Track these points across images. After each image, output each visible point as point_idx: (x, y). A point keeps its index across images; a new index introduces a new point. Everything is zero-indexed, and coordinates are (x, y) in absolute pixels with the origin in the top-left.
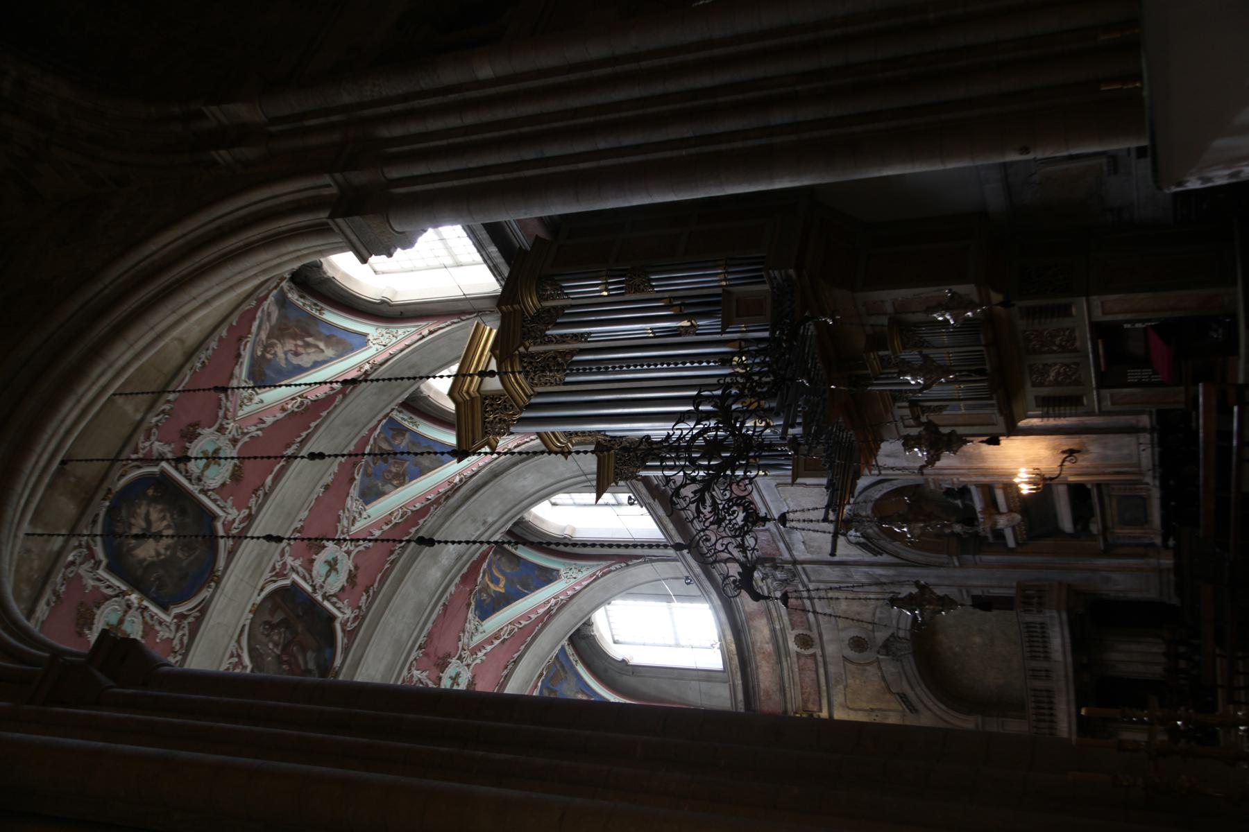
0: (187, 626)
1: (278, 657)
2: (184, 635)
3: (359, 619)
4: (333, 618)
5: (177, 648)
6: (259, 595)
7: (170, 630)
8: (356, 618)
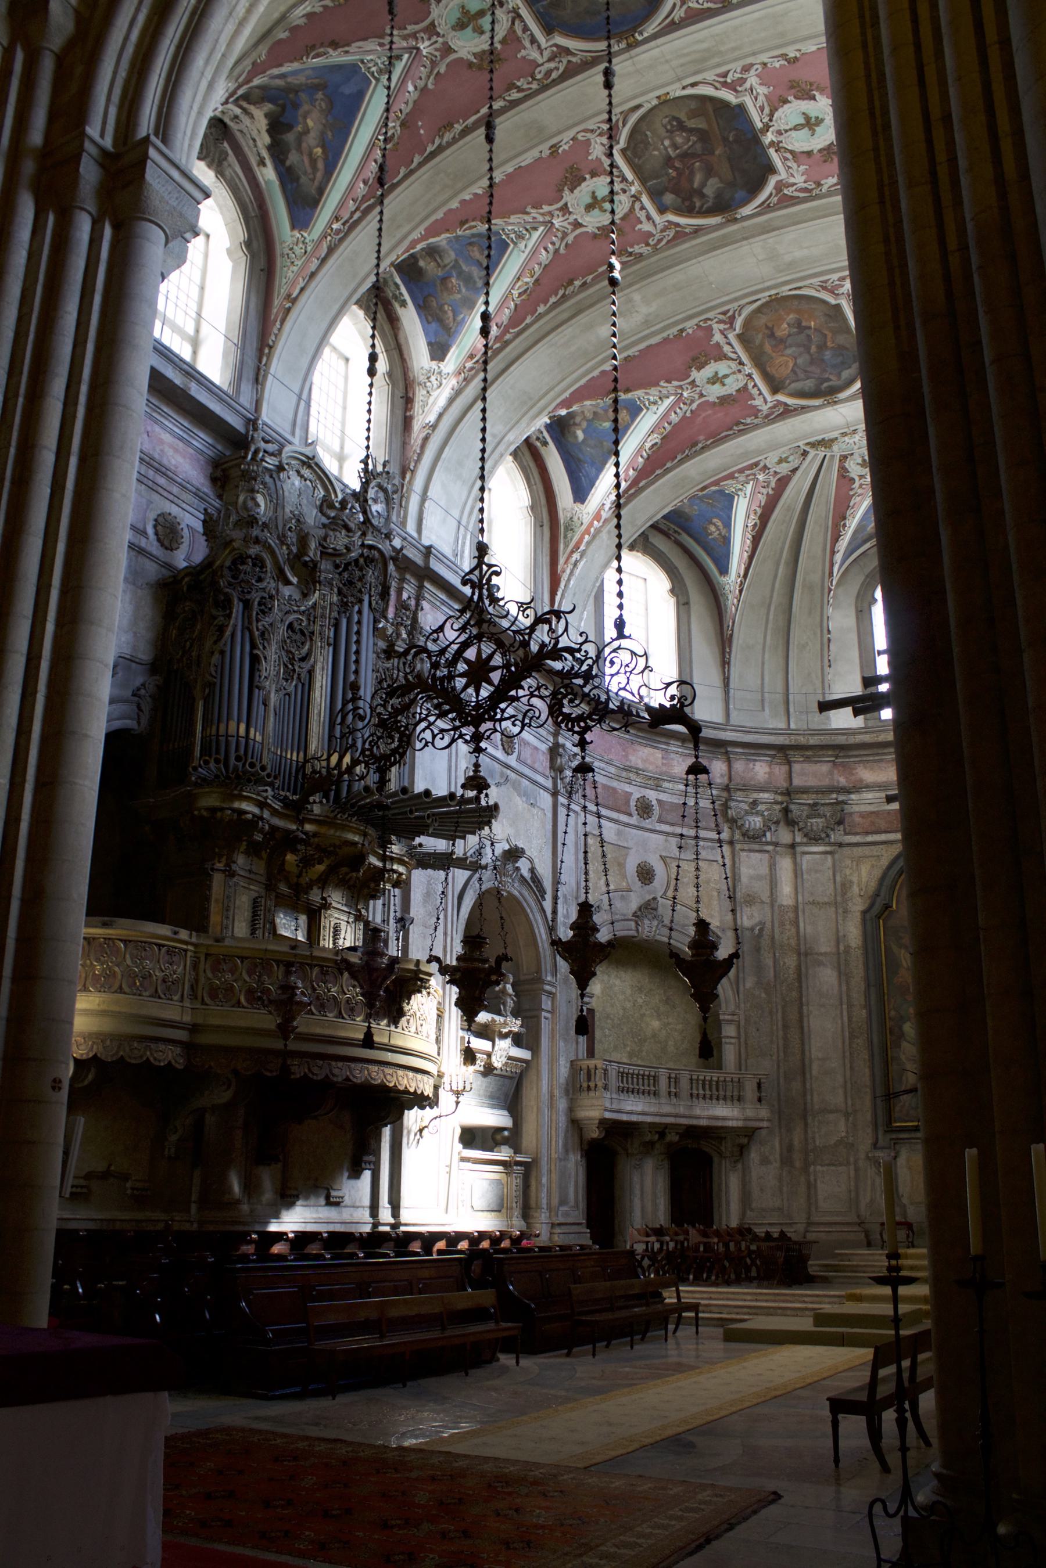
0: (565, 62)
2: (557, 69)
4: (771, 170)
5: (539, 77)
6: (684, 88)
7: (542, 54)
8: (806, 190)
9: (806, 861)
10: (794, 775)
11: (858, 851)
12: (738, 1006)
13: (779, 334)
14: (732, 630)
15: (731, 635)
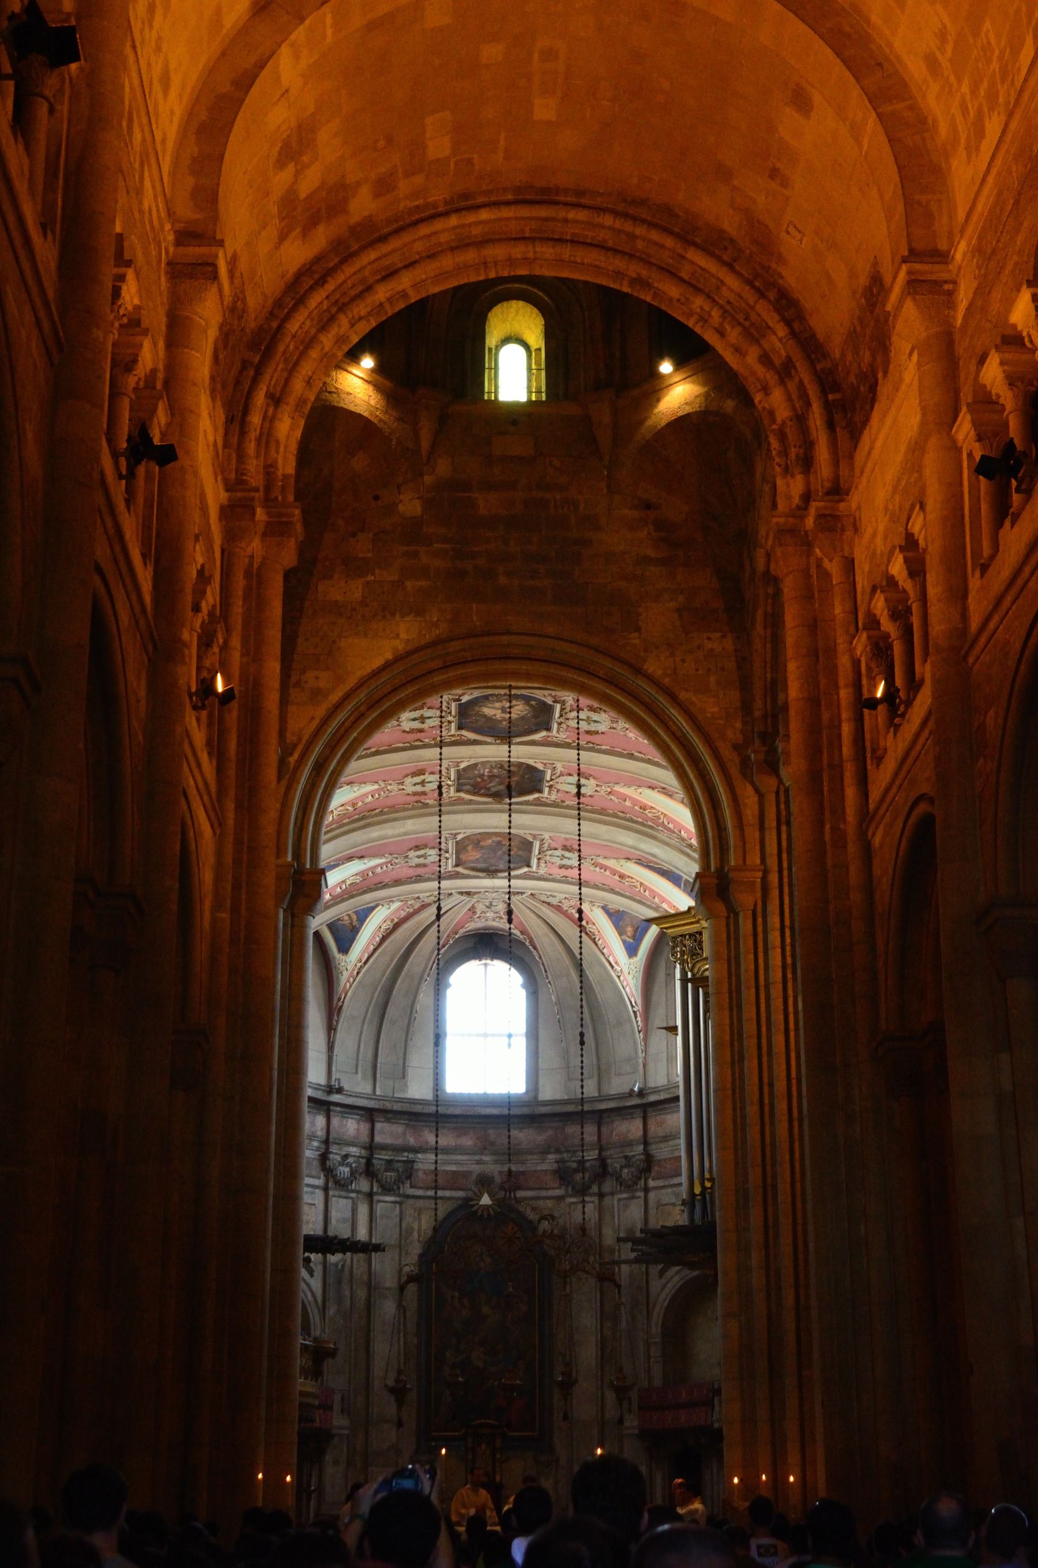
1: (483, 775)
3: (554, 805)
4: (540, 791)
9: (379, 1208)
10: (376, 1132)
11: (420, 1203)
12: (323, 1330)
13: (481, 844)
14: (343, 1002)
15: (341, 1007)
